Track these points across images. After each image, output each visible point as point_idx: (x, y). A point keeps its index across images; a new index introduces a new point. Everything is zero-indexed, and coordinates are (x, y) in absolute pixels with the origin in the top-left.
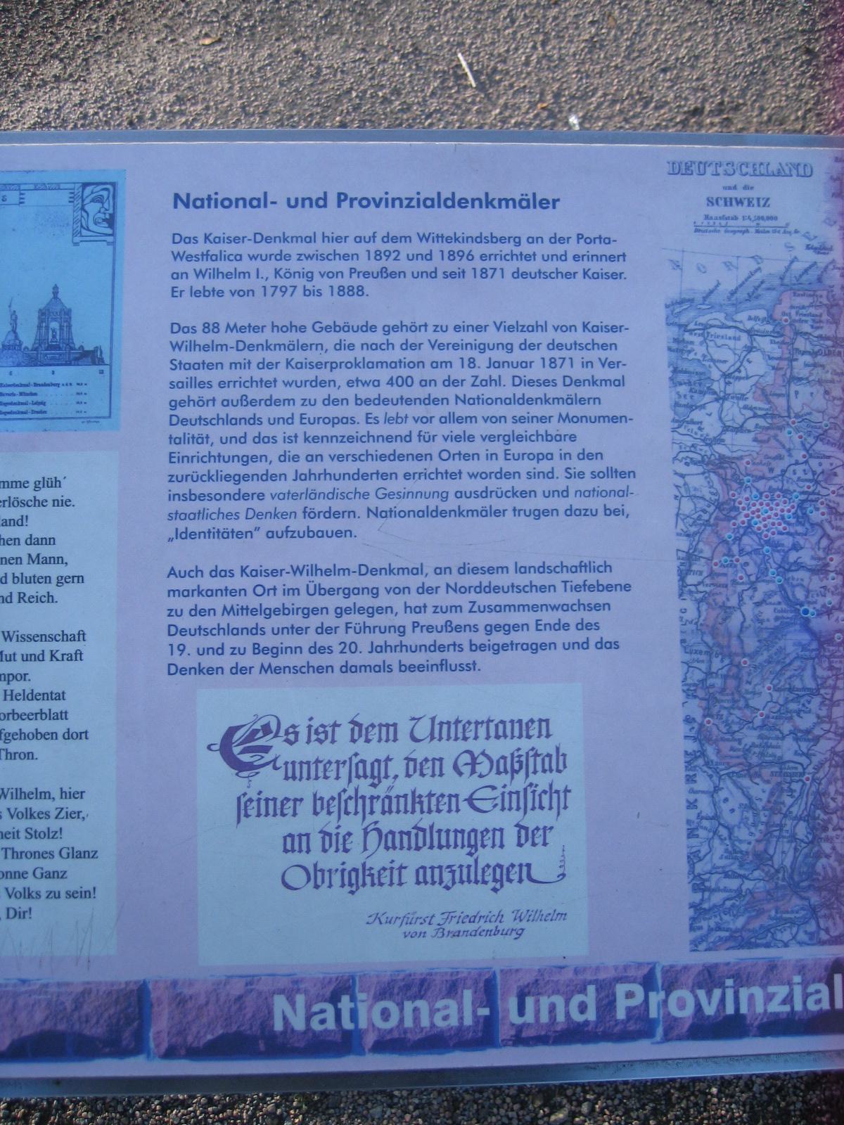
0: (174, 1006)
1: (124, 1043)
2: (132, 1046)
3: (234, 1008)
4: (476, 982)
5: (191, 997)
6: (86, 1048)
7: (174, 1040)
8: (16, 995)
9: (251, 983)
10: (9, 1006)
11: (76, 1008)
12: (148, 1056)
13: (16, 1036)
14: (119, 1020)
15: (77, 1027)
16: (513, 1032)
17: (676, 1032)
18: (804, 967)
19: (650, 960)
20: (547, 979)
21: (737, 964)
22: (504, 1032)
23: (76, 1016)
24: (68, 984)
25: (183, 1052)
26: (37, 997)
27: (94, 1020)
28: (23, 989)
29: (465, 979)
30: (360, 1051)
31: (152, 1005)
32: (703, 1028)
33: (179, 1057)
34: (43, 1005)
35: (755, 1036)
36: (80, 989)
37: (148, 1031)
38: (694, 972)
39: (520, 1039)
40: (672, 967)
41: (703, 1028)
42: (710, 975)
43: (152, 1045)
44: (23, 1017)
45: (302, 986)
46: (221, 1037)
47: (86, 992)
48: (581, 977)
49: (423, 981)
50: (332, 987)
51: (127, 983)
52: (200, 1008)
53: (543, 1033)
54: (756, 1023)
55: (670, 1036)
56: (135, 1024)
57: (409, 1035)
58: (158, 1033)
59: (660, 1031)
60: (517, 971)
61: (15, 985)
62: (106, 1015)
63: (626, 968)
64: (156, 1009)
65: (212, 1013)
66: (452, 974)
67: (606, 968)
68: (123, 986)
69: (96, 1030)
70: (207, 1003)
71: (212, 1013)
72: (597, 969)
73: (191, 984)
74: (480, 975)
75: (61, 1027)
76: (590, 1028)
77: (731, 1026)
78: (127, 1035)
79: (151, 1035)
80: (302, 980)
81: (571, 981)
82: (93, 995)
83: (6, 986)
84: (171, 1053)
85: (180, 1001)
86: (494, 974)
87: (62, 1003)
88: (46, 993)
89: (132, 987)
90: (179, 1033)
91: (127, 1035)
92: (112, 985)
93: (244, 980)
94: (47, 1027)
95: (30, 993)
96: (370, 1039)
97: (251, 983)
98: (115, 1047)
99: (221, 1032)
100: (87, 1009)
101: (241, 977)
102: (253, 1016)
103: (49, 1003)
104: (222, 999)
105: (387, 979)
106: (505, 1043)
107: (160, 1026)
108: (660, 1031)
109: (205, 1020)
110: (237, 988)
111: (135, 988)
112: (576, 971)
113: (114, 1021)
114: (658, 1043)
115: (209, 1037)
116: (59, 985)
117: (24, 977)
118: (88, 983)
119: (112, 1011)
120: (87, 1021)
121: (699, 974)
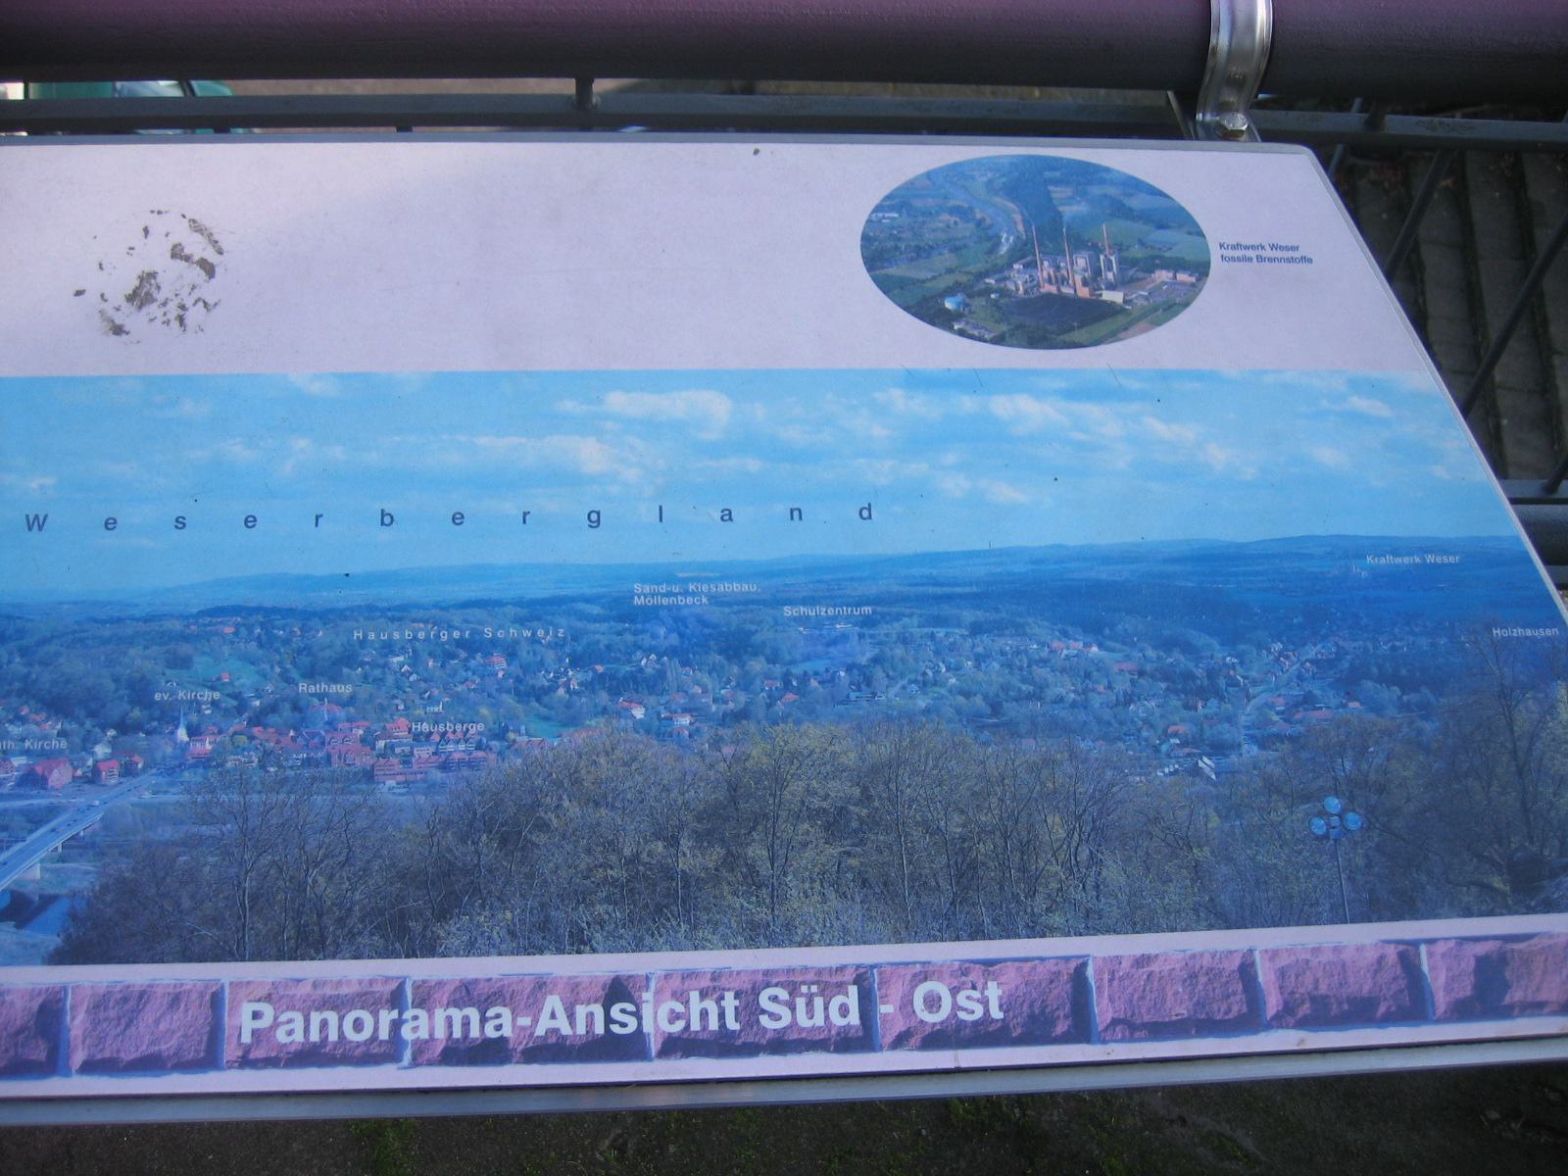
4: (201, 995)
16: (240, 1053)
18: (577, 985)
19: (400, 974)
21: (501, 980)
22: (230, 1052)
29: (190, 991)
30: (67, 1073)
32: (458, 1053)
35: (518, 1063)
39: (245, 1062)
40: (424, 982)
41: (458, 1053)
42: (467, 990)
48: (319, 992)
49: (142, 994)
54: (521, 1048)
55: (420, 1061)
57: (122, 1055)
60: (248, 983)
63: (371, 982)
66: (175, 986)
67: (349, 982)
72: (339, 983)
74: (206, 987)
77: (492, 1051)
80: (9, 991)
81: (309, 996)
86: (222, 987)
96: (79, 1057)
105: (102, 991)
106: (230, 1066)
112: (315, 985)
114: (405, 1068)
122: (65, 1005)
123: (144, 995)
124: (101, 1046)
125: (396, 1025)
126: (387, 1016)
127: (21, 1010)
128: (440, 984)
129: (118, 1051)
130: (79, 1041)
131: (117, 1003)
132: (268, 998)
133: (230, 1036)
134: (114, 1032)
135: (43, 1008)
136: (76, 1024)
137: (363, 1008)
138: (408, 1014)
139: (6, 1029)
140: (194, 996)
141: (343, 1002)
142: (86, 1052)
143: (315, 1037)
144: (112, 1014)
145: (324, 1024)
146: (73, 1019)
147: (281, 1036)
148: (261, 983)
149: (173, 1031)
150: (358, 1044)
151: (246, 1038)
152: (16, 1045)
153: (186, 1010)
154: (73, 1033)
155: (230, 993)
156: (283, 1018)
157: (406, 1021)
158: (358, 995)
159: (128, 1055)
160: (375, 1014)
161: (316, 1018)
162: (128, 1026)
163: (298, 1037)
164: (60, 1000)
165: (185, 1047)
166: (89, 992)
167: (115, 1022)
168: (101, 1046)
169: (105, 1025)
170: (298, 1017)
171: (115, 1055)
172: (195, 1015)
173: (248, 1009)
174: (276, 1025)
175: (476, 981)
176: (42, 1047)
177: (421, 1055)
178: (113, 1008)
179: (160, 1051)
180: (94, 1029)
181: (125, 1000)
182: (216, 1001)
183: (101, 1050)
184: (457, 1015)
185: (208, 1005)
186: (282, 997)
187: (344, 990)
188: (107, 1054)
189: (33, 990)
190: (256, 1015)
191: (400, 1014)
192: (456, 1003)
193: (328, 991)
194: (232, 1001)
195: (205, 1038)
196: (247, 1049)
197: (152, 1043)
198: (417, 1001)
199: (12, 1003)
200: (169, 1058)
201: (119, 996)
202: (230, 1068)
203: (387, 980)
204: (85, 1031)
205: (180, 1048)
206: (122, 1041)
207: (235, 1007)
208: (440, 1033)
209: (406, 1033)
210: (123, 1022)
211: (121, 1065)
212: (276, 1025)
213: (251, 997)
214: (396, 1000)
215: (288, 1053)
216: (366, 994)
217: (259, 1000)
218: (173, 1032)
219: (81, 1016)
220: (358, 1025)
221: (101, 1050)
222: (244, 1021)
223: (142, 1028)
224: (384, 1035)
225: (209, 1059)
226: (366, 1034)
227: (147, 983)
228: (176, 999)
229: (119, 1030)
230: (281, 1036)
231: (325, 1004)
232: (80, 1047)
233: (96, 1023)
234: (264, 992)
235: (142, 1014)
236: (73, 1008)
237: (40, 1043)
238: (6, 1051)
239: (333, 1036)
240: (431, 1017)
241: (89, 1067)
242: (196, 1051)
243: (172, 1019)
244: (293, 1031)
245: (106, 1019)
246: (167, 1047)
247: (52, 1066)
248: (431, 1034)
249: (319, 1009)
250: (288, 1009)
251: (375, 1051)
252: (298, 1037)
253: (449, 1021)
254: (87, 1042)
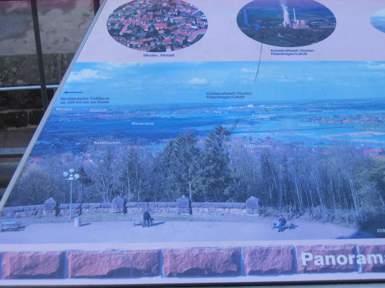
0: (172, 258)
1: (153, 272)
2: (156, 272)
3: (195, 259)
4: (287, 250)
5: (178, 255)
6: (138, 273)
7: (172, 271)
8: (111, 255)
9: (201, 250)
10: (108, 258)
11: (134, 259)
12: (162, 276)
13: (110, 269)
14: (150, 264)
15: (134, 266)
16: (303, 268)
17: (367, 270)
20: (315, 249)
22: (300, 268)
23: (134, 262)
24: (131, 251)
25: (176, 275)
26: (118, 255)
27: (141, 263)
28: (114, 253)
29: (283, 249)
30: (245, 275)
31: (163, 258)
33: (174, 276)
34: (121, 258)
36: (136, 252)
37: (162, 268)
38: (371, 248)
39: (305, 271)
40: (363, 246)
42: (378, 249)
43: (163, 272)
44: (113, 263)
45: (221, 251)
46: (191, 269)
47: (138, 253)
49: (267, 250)
50: (232, 252)
51: (154, 250)
52: (182, 259)
53: (315, 269)
55: (365, 271)
56: (157, 265)
57: (263, 269)
58: (166, 268)
59: (360, 269)
60: (303, 246)
61: (110, 251)
62: (145, 262)
63: (345, 246)
64: (165, 259)
65: (186, 261)
66: (278, 247)
67: (337, 246)
68: (152, 251)
69: (142, 267)
70: (185, 257)
71: (186, 261)
72: (334, 247)
73: (178, 250)
74: (289, 248)
75: (128, 266)
76: (333, 267)
78: (153, 269)
79: (163, 269)
80: (221, 249)
81: (324, 250)
82: (140, 254)
83: (107, 251)
84: (171, 275)
85: (174, 257)
86: (294, 248)
87: (129, 258)
88: (122, 254)
89: (155, 252)
90: (174, 268)
91: (153, 269)
92: (148, 251)
93: (198, 250)
94: (122, 266)
95: (116, 254)
96: (248, 270)
97: (201, 250)
98: (149, 273)
99: (190, 267)
100: (138, 259)
101: (197, 248)
102: (203, 262)
103: (124, 257)
104: (190, 255)
105: (253, 249)
106: (300, 272)
107: (167, 265)
108: (360, 269)
109: (184, 263)
110: (196, 252)
111: (157, 252)
113: (149, 264)
114: (360, 273)
115: (186, 269)
116: (127, 251)
117: (114, 248)
118: (138, 250)
119: (148, 260)
120: (138, 264)
121: (374, 248)
122: (241, 253)
123: (268, 250)
124: (255, 267)
125: (355, 260)
126: (351, 257)
127: (226, 255)
128: (368, 247)
129: (261, 268)
130: (248, 264)
131: (259, 252)
132: (310, 251)
133: (299, 263)
134: (259, 262)
135: (233, 254)
136: (246, 259)
137: (343, 254)
138: (358, 256)
139: (221, 261)
140: (285, 251)
141: (336, 252)
142: (250, 268)
143: (328, 263)
144: (258, 256)
145: (330, 260)
146: (244, 258)
147: (316, 263)
148: (307, 247)
149: (281, 262)
150: (343, 266)
151: (304, 264)
152: (226, 266)
153: (283, 255)
154: (245, 262)
155: (297, 249)
156: (316, 257)
157: (358, 258)
158: (341, 250)
159: (265, 269)
160: (347, 256)
161: (327, 258)
162: (264, 260)
163: (322, 263)
164: (239, 252)
165: (284, 267)
166: (249, 249)
167: (259, 259)
168: (255, 267)
169: (256, 260)
170: (321, 257)
171: (260, 269)
172: (287, 257)
173: (303, 255)
174: (314, 260)
175: (380, 246)
176: (235, 267)
177: (365, 269)
178: (258, 254)
179: (276, 268)
180: (252, 261)
181: (261, 252)
182: (293, 252)
183: (255, 268)
184: (375, 256)
185: (290, 253)
186: (315, 251)
187: (336, 249)
188: (258, 269)
189: (229, 249)
190: (307, 257)
191: (356, 256)
192: (375, 253)
193: (331, 249)
194: (298, 252)
195: (291, 264)
196: (306, 268)
197: (273, 265)
198: (361, 252)
199: (223, 253)
200: (279, 270)
201: (259, 251)
202: (300, 273)
203: (350, 245)
204: (249, 261)
205: (282, 267)
206: (262, 265)
207: (300, 254)
208: (370, 262)
209: (358, 262)
210: (262, 259)
211: (263, 272)
212: (314, 260)
213: (305, 251)
214: (354, 251)
215: (320, 268)
216: (343, 250)
217: (308, 252)
218: (279, 262)
219: (247, 257)
220: (342, 260)
221: (255, 268)
222: (303, 259)
223: (268, 260)
224: (351, 262)
225: (293, 270)
226: (345, 262)
227: (269, 246)
228: (279, 252)
229: (261, 261)
230: (316, 263)
231: (330, 253)
232: (248, 267)
233: (252, 259)
234: (309, 249)
235: (267, 257)
236: (244, 254)
237: (234, 265)
238: (223, 268)
239: (334, 263)
240: (366, 257)
241: (252, 273)
242: (288, 268)
243: (278, 258)
244: (320, 261)
245: (256, 258)
246: (278, 267)
247: (239, 272)
248: (367, 263)
249: (328, 254)
250: (318, 255)
251: (350, 267)
252: (322, 263)
253: (372, 258)
254: (250, 265)
